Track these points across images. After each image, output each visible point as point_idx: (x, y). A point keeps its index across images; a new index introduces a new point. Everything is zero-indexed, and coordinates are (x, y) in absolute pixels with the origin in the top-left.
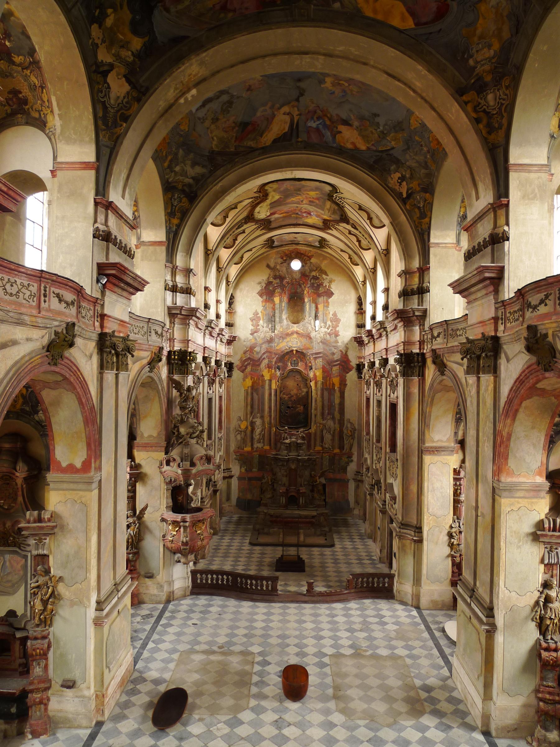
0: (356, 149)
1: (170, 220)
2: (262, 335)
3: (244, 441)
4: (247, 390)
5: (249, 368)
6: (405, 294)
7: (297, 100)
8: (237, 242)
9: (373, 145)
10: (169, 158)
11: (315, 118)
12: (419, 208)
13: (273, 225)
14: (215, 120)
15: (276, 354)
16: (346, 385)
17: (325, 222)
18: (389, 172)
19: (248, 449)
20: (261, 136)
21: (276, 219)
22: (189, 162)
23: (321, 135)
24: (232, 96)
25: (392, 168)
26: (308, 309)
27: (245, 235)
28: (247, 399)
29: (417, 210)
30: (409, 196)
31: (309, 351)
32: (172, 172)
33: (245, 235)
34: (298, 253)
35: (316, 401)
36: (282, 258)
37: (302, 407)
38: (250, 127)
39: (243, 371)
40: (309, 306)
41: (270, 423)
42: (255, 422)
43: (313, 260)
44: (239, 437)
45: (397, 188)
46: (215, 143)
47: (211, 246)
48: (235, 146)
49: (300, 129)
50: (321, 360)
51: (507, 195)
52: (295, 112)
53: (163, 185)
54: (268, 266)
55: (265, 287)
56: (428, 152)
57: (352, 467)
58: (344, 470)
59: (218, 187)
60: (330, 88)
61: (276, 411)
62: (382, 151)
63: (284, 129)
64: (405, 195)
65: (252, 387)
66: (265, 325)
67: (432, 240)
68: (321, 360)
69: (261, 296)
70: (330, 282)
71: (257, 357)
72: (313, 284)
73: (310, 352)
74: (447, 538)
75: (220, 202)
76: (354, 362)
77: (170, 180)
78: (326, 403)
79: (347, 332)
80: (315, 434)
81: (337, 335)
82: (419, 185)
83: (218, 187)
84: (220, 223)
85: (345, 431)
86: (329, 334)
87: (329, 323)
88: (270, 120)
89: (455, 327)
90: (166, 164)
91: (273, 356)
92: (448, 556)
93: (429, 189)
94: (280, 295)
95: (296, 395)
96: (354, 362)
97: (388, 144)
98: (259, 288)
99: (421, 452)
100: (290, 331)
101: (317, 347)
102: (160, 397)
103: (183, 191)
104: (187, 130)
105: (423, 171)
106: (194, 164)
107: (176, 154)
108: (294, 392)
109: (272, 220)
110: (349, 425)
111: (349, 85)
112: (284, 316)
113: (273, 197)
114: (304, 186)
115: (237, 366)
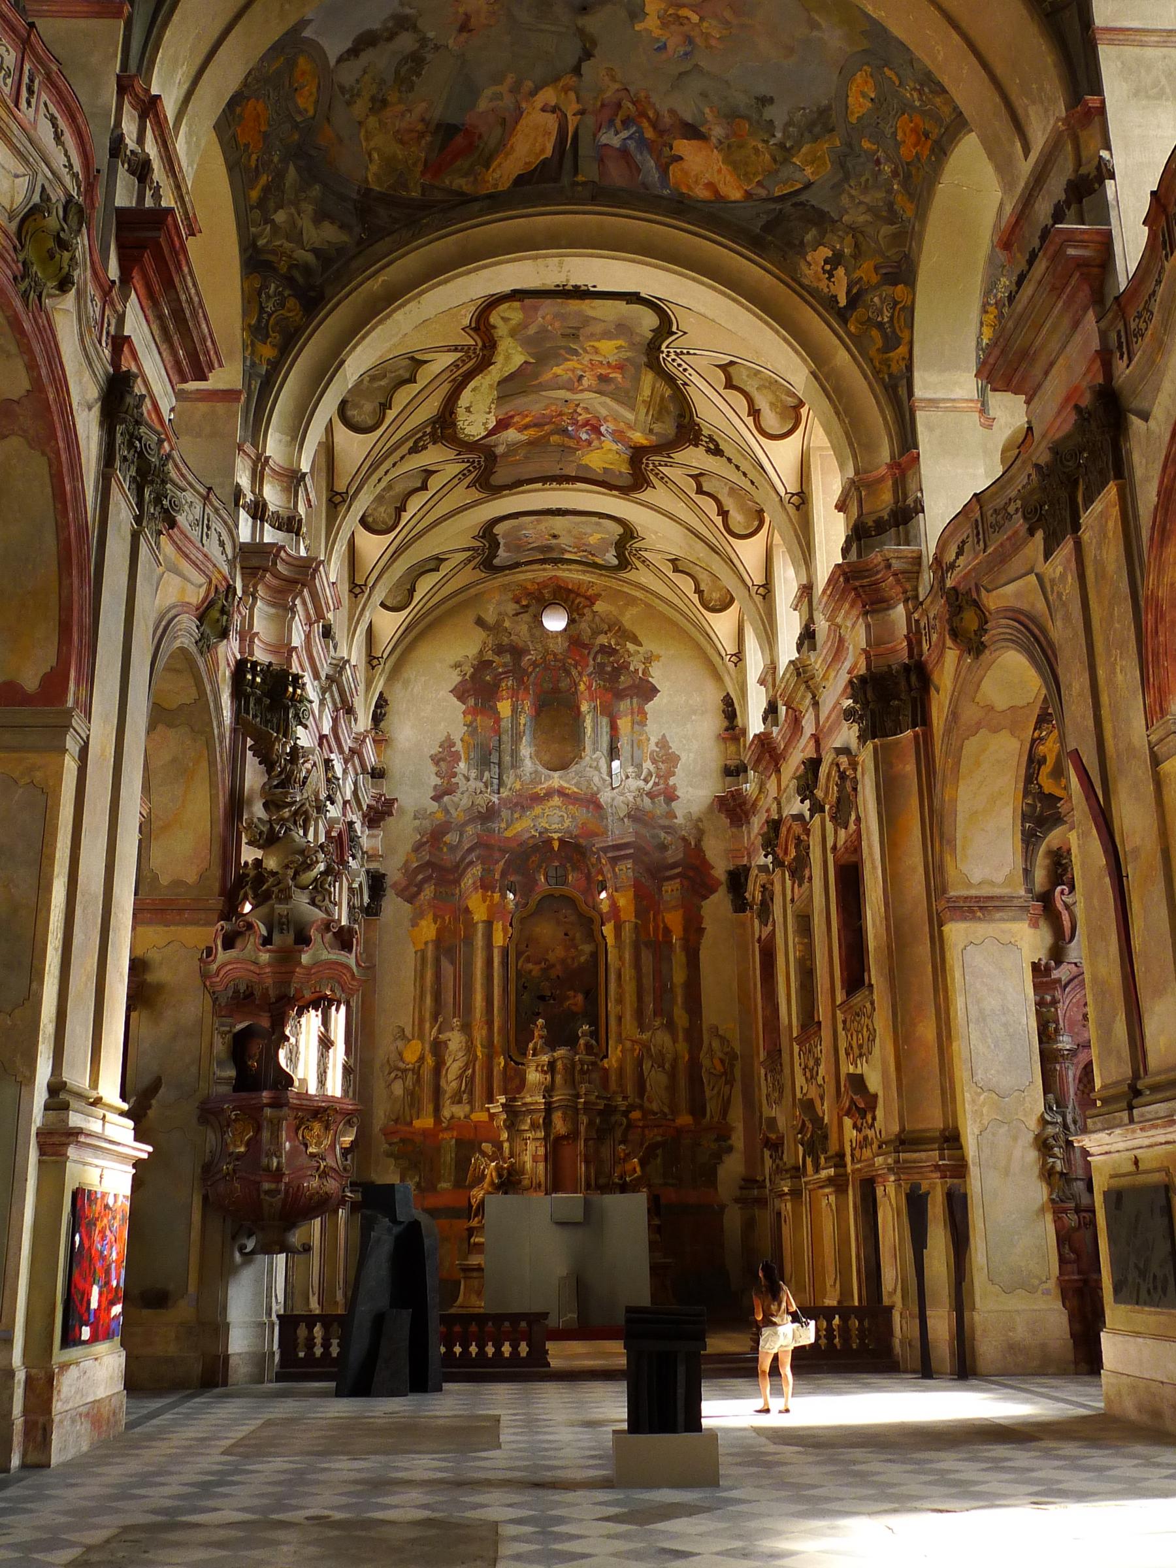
0: (719, 198)
1: (253, 344)
2: (465, 802)
3: (413, 1098)
4: (423, 952)
5: (428, 892)
6: (861, 535)
7: (577, 71)
8: (406, 517)
9: (759, 183)
10: (263, 180)
11: (618, 122)
12: (880, 326)
13: (501, 476)
14: (379, 104)
15: (503, 851)
16: (701, 931)
17: (638, 455)
18: (800, 249)
19: (425, 1122)
20: (488, 167)
21: (513, 448)
22: (308, 208)
23: (634, 167)
24: (423, 42)
25: (808, 237)
26: (589, 731)
27: (429, 494)
28: (422, 977)
29: (875, 333)
30: (854, 300)
31: (596, 840)
32: (266, 223)
33: (429, 494)
34: (560, 587)
35: (619, 976)
36: (517, 602)
37: (580, 998)
38: (460, 140)
39: (410, 900)
40: (593, 727)
41: (489, 1044)
42: (445, 1043)
43: (599, 606)
44: (398, 1089)
45: (823, 285)
46: (374, 168)
47: (341, 486)
48: (423, 186)
49: (582, 152)
50: (629, 864)
51: (1098, 89)
52: (571, 107)
53: (243, 250)
54: (480, 622)
55: (473, 676)
56: (895, 173)
57: (732, 1167)
58: (709, 1176)
59: (375, 285)
60: (657, 32)
61: (505, 1007)
62: (782, 198)
63: (543, 151)
64: (843, 302)
65: (438, 942)
66: (473, 774)
67: (918, 392)
68: (629, 864)
69: (461, 698)
70: (648, 660)
71: (449, 859)
72: (601, 666)
73: (599, 843)
74: (1033, 1155)
75: (380, 322)
76: (720, 869)
77: (261, 242)
78: (648, 982)
79: (695, 791)
80: (621, 1070)
81: (671, 797)
82: (876, 268)
83: (375, 285)
84: (370, 422)
85: (706, 1062)
86: (650, 795)
87: (648, 765)
88: (508, 123)
89: (1000, 502)
90: (254, 194)
91: (497, 855)
92: (1042, 1210)
93: (902, 272)
94: (514, 694)
95: (563, 961)
96: (720, 869)
97: (798, 175)
98: (455, 678)
99: (936, 924)
100: (540, 789)
101: (619, 831)
102: (212, 763)
103: (289, 280)
104: (311, 113)
105: (886, 230)
106: (320, 216)
107: (280, 175)
108: (560, 952)
109: (500, 450)
110: (716, 1044)
111: (702, 19)
112: (526, 750)
113: (508, 358)
114: (587, 321)
115: (394, 886)
